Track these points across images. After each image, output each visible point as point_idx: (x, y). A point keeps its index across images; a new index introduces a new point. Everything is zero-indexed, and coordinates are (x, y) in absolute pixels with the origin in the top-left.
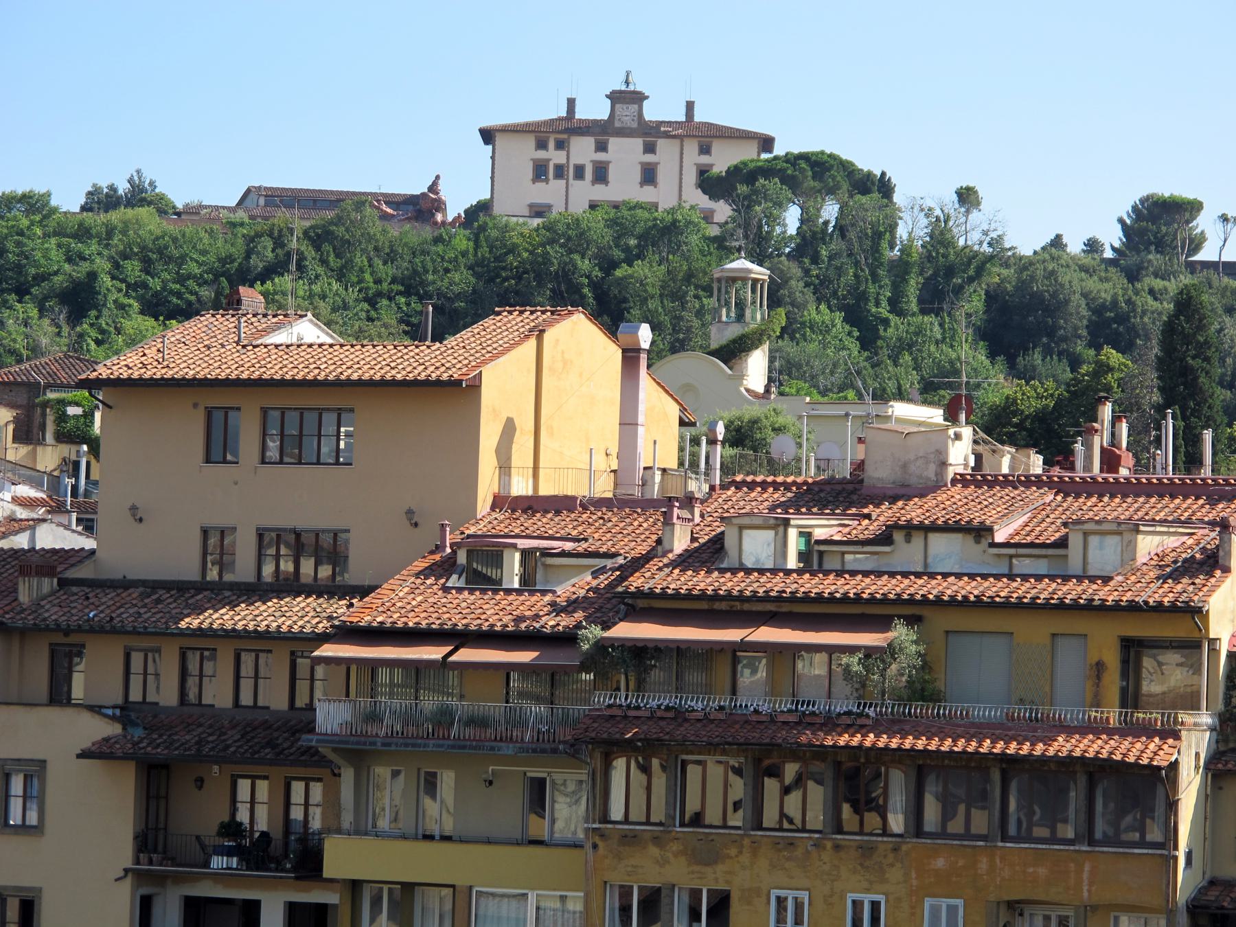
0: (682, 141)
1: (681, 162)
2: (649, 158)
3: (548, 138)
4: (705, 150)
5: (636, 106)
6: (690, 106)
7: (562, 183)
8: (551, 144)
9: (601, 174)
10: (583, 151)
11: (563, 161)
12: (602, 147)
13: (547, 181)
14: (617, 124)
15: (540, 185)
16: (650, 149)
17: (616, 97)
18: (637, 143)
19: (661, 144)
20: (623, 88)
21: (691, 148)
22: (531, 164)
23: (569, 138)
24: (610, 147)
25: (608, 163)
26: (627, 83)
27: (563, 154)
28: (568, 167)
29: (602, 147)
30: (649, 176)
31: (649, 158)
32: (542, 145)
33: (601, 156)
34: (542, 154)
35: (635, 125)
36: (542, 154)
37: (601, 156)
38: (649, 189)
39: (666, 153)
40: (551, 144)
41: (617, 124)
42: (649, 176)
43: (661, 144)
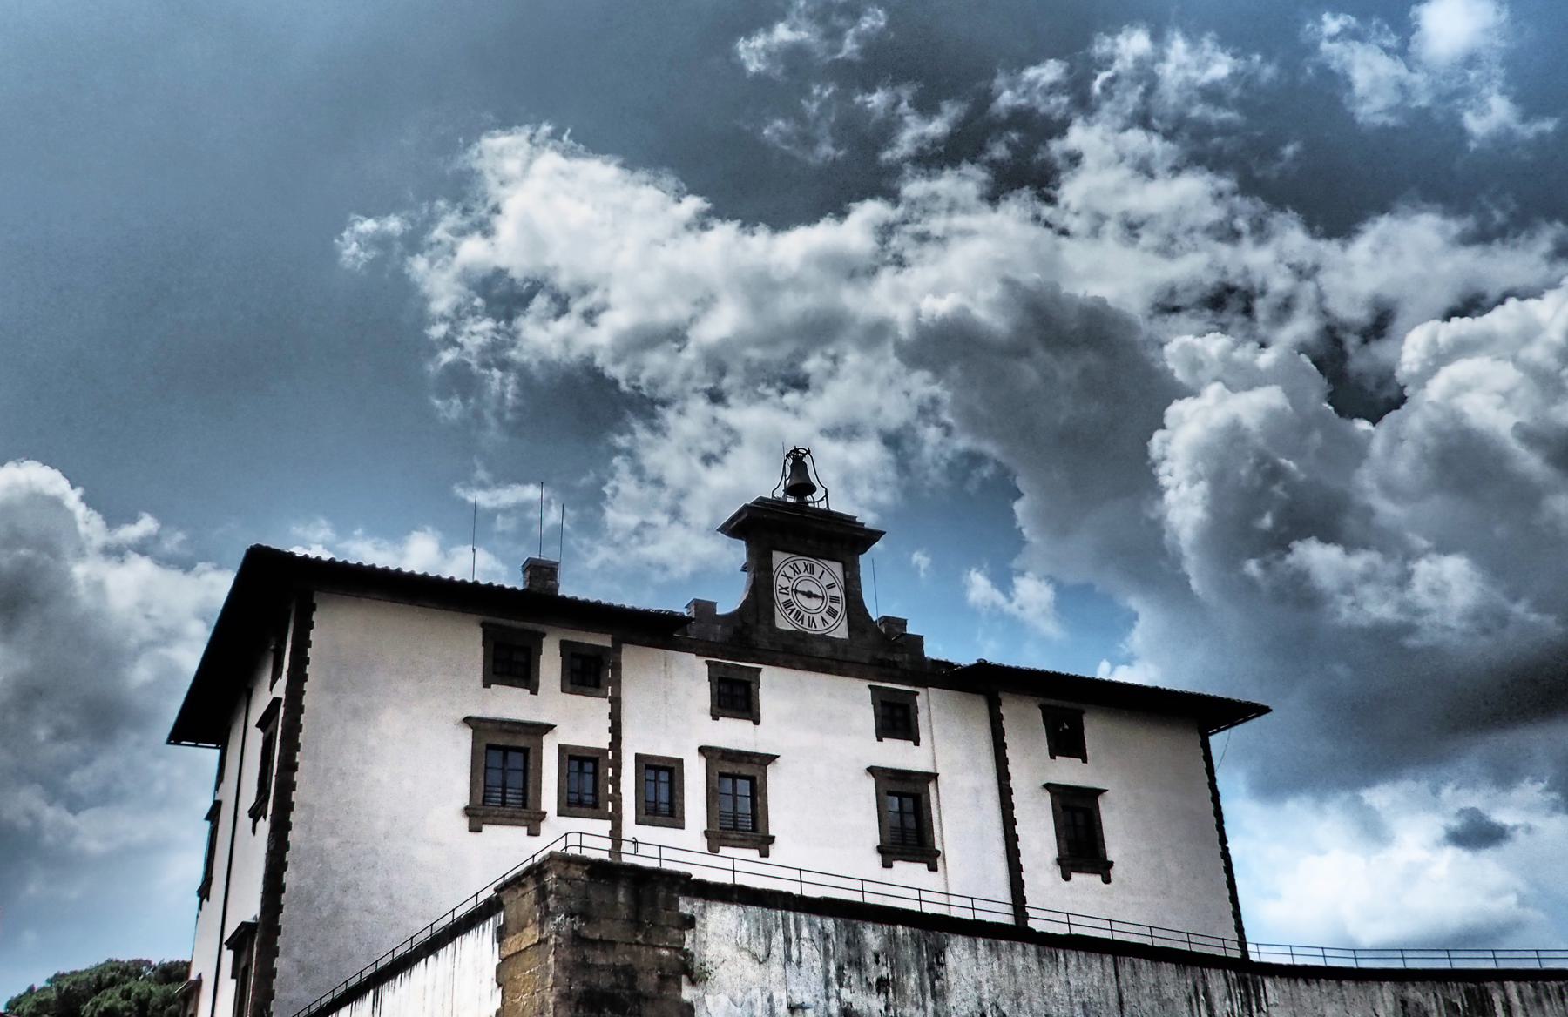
1: (1003, 777)
5: (836, 567)
8: (550, 665)
13: (533, 821)
14: (783, 622)
19: (931, 705)
22: (464, 740)
23: (617, 649)
24: (768, 700)
26: (801, 486)
27: (602, 707)
28: (617, 765)
31: (898, 755)
33: (734, 734)
34: (510, 704)
35: (841, 632)
36: (510, 704)
37: (734, 734)
38: (909, 873)
40: (550, 665)
41: (783, 622)
43: (931, 705)
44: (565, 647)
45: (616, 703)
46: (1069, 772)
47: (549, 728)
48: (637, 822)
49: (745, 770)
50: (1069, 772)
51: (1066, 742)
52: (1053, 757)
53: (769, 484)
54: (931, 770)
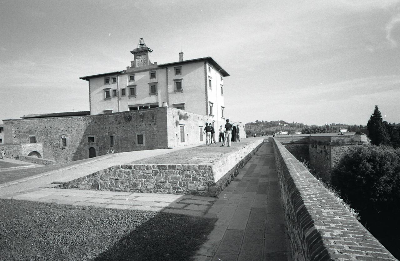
0: (167, 69)
1: (167, 80)
2: (154, 80)
3: (109, 78)
4: (178, 72)
6: (181, 54)
7: (116, 99)
9: (133, 91)
10: (124, 82)
11: (116, 88)
12: (132, 78)
15: (108, 101)
16: (153, 76)
17: (136, 53)
18: (147, 75)
20: (139, 47)
21: (171, 71)
25: (135, 85)
27: (116, 84)
29: (132, 78)
30: (153, 89)
31: (154, 80)
32: (107, 82)
34: (107, 86)
36: (107, 86)
39: (161, 76)
42: (153, 89)
44: (112, 78)
45: (118, 82)
46: (178, 77)
47: (110, 88)
48: (121, 96)
49: (133, 87)
50: (178, 77)
51: (178, 72)
52: (175, 75)
53: (137, 46)
54: (156, 81)
